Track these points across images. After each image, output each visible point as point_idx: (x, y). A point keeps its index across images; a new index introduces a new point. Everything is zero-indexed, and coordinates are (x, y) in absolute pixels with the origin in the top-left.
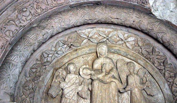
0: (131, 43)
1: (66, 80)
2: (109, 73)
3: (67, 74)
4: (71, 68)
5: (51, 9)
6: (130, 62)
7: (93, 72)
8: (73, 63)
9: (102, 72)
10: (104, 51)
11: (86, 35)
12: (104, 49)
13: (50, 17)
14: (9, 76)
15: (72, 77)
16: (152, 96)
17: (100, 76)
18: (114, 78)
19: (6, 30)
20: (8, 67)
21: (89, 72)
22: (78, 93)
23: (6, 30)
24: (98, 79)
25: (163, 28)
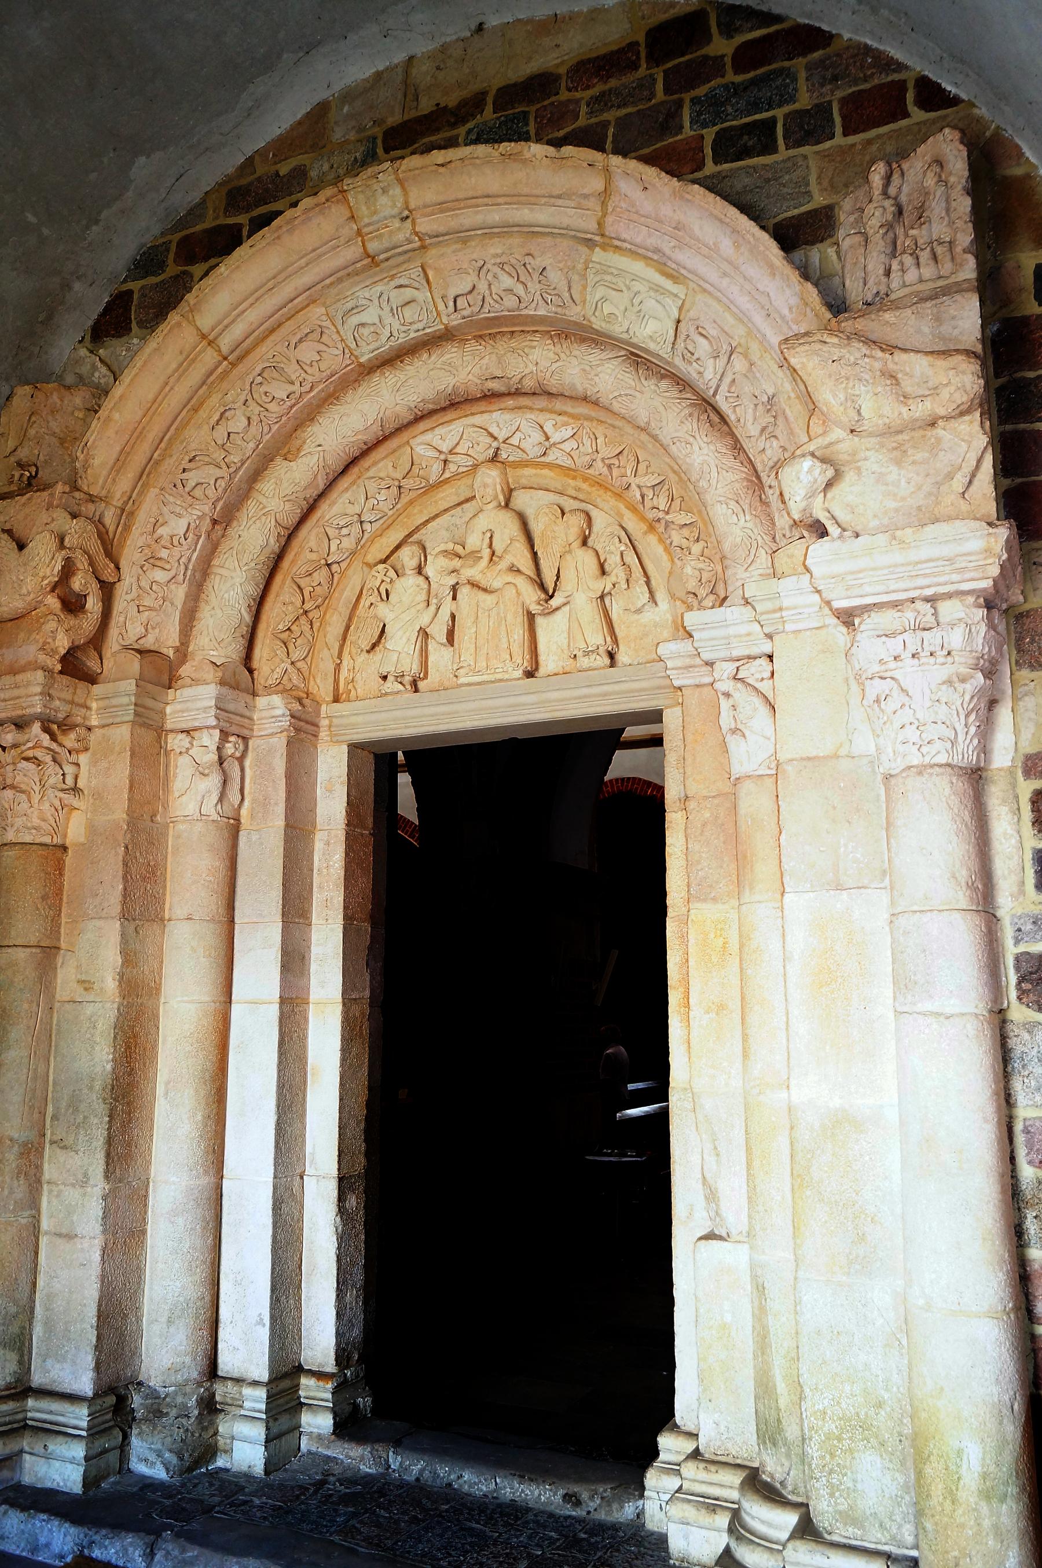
0: (567, 447)
7: (456, 563)
10: (490, 491)
12: (489, 481)
13: (310, 415)
14: (213, 612)
15: (410, 582)
23: (191, 483)
24: (474, 585)
25: (627, 380)
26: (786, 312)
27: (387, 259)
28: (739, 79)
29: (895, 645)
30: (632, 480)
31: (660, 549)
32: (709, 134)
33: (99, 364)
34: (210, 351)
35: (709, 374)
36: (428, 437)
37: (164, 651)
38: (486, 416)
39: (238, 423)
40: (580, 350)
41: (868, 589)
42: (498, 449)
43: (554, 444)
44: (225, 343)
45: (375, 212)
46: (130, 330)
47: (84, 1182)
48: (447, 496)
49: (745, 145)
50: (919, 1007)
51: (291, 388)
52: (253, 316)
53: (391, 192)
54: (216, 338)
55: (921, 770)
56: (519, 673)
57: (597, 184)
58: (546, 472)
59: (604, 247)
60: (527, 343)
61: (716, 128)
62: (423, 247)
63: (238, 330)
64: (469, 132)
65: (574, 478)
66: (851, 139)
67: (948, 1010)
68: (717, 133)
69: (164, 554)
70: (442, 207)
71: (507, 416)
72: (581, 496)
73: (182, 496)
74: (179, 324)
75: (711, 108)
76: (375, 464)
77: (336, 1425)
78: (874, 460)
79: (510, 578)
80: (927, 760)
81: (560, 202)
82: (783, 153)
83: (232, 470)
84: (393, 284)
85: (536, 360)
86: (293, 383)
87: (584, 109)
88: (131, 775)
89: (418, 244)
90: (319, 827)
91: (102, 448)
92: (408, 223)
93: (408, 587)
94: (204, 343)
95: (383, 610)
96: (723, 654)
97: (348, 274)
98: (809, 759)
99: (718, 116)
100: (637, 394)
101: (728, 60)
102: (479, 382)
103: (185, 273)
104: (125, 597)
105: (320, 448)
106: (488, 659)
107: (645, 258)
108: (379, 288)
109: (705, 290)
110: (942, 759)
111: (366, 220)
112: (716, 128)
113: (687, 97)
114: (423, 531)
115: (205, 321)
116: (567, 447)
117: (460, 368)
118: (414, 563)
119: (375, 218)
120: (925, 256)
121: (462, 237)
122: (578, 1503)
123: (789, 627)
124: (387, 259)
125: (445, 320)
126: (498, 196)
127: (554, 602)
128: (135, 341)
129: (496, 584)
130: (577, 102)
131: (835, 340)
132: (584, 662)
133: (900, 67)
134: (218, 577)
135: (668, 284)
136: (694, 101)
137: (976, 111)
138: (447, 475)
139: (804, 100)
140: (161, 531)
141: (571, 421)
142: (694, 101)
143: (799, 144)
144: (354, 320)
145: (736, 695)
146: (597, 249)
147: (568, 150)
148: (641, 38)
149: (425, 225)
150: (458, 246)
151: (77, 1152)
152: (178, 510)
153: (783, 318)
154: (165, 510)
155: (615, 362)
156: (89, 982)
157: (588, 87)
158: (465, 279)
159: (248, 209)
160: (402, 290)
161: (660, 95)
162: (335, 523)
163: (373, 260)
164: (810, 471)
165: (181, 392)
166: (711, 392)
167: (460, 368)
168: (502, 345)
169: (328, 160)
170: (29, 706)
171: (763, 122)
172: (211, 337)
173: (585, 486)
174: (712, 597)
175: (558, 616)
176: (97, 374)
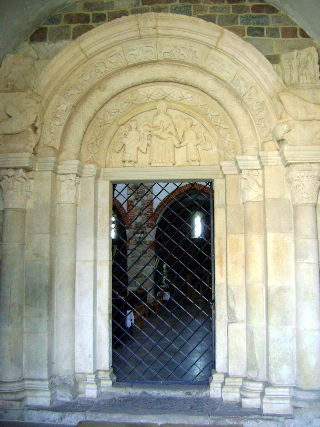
0: (189, 100)
1: (128, 137)
2: (166, 129)
3: (129, 131)
4: (133, 124)
5: (110, 71)
8: (135, 120)
10: (163, 109)
11: (145, 93)
13: (109, 77)
16: (207, 151)
17: (158, 132)
18: (171, 133)
19: (69, 94)
21: (148, 128)
22: (138, 148)
23: (69, 94)
24: (157, 136)
26: (272, 82)
27: (145, 38)
28: (254, 14)
29: (302, 173)
32: (246, 27)
33: (32, 49)
34: (83, 55)
36: (143, 89)
37: (56, 147)
38: (163, 86)
39: (87, 77)
40: (201, 75)
41: (297, 159)
42: (166, 97)
43: (185, 98)
44: (88, 53)
46: (46, 40)
47: (40, 315)
48: (147, 107)
49: (256, 33)
50: (305, 261)
51: (106, 69)
52: (100, 46)
53: (152, 21)
54: (85, 51)
55: (306, 205)
56: (172, 165)
57: (218, 35)
58: (180, 105)
59: (215, 50)
60: (184, 70)
61: (248, 26)
62: (157, 37)
63: (93, 49)
64: (172, 6)
65: (189, 109)
66: (284, 39)
67: (311, 262)
68: (248, 27)
69: (59, 116)
70: (168, 28)
71: (170, 87)
72: (190, 114)
73: (66, 98)
74: (75, 45)
75: (247, 20)
76: (124, 95)
77: (113, 384)
78: (298, 126)
79: (170, 136)
80: (308, 202)
82: (266, 38)
83: (82, 92)
85: (187, 75)
86: (106, 68)
87: (209, 10)
88: (51, 188)
90: (99, 207)
91: (44, 80)
92: (155, 30)
93: (133, 134)
94: (81, 52)
95: (124, 140)
96: (246, 168)
98: (273, 199)
99: (249, 23)
101: (250, 8)
103: (68, 26)
104: (46, 129)
106: (162, 159)
107: (227, 56)
108: (141, 45)
109: (245, 69)
110: (311, 202)
111: (142, 26)
112: (248, 26)
113: (239, 15)
114: (136, 117)
115: (83, 45)
116: (189, 100)
117: (162, 72)
118: (135, 127)
120: (308, 77)
121: (170, 36)
122: (190, 394)
123: (269, 164)
124: (145, 38)
125: (159, 58)
126: (186, 29)
127: (182, 145)
128: (47, 44)
129: (165, 137)
130: (207, 7)
131: (292, 95)
132: (192, 163)
133: (295, 24)
134: (75, 125)
135: (234, 65)
136: (241, 17)
137: (314, 41)
138: (147, 101)
139: (271, 25)
140: (58, 108)
141: (191, 93)
142: (241, 17)
143: (270, 36)
144: (130, 53)
145: (249, 179)
146: (213, 50)
149: (160, 31)
151: (36, 307)
152: (64, 102)
153: (270, 83)
154: (60, 102)
155: (212, 81)
156: (38, 254)
157: (209, 4)
159: (92, 11)
160: (148, 47)
161: (231, 13)
163: (140, 37)
164: (287, 127)
165: (70, 66)
166: (242, 95)
168: (176, 69)
169: (122, 2)
170: (23, 164)
171: (261, 28)
172: (84, 50)
173: (192, 112)
174: (233, 150)
175: (182, 149)
176: (31, 52)
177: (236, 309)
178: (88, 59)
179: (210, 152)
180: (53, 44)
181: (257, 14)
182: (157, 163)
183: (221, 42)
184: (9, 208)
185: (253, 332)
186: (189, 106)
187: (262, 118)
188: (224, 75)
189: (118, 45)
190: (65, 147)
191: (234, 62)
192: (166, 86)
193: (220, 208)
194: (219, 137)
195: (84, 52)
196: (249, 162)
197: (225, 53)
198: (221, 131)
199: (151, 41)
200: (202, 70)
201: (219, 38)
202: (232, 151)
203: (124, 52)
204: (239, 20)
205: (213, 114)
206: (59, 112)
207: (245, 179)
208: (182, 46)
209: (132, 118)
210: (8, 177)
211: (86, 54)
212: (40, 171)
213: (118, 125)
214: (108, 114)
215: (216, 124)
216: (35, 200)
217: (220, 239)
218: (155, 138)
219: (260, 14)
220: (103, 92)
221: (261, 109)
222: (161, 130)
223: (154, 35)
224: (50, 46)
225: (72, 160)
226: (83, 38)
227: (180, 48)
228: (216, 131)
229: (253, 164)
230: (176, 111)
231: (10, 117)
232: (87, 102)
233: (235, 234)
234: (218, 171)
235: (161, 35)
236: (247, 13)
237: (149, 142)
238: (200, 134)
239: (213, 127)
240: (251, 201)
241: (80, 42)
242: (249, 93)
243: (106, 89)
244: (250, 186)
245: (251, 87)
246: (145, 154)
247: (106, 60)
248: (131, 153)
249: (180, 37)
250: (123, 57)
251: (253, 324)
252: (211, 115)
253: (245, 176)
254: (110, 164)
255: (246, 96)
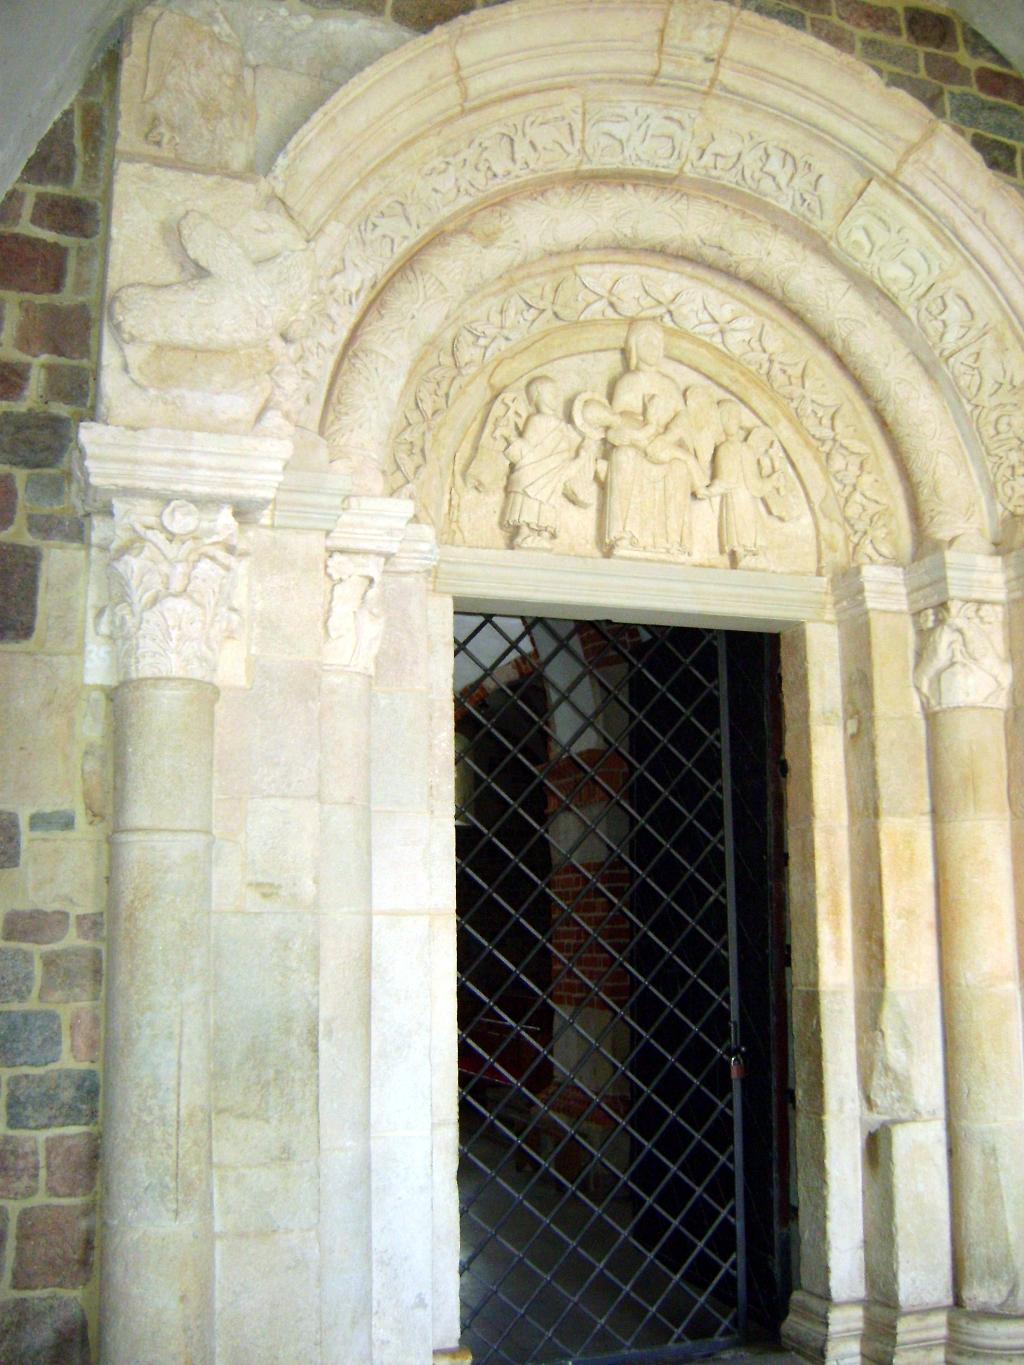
1: (529, 434)
4: (548, 395)
6: (730, 401)
9: (645, 423)
19: (379, 232)
20: (373, 371)
24: (633, 445)
27: (664, 85)
28: (983, 96)
30: (807, 394)
31: (816, 468)
34: (455, 88)
35: (951, 337)
36: (597, 269)
38: (662, 273)
44: (476, 86)
45: (689, 39)
53: (714, 31)
58: (703, 351)
59: (883, 183)
63: (495, 79)
65: (732, 368)
70: (756, 72)
72: (734, 388)
74: (441, 45)
79: (679, 454)
81: (869, 129)
84: (665, 113)
89: (703, 88)
92: (711, 66)
93: (547, 427)
96: (964, 594)
97: (624, 80)
100: (868, 325)
102: (699, 243)
105: (517, 245)
106: (654, 536)
108: (650, 109)
111: (676, 42)
113: (947, 88)
115: (466, 53)
116: (739, 336)
117: (691, 222)
119: (687, 45)
121: (749, 104)
126: (814, 92)
129: (664, 456)
135: (938, 247)
141: (752, 314)
147: (901, 93)
148: (900, 10)
149: (727, 76)
150: (740, 110)
156: (271, 885)
157: (858, 25)
158: (729, 139)
160: (668, 123)
162: (480, 329)
166: (946, 353)
167: (691, 222)
170: (255, 487)
173: (742, 379)
174: (885, 530)
177: (914, 1073)
178: (464, 113)
179: (789, 528)
180: (307, 20)
181: (991, 99)
182: (633, 544)
183: (916, 162)
184: (146, 679)
185: (994, 1150)
186: (732, 360)
187: (1011, 435)
188: (893, 274)
189: (570, 86)
190: (343, 441)
191: (938, 239)
192: (671, 275)
193: (826, 724)
194: (828, 480)
195: (461, 80)
196: (975, 576)
197: (915, 202)
198: (838, 463)
199: (682, 102)
200: (821, 247)
201: (912, 148)
202: (881, 533)
203: (588, 117)
204: (946, 98)
205: (820, 398)
206: (336, 295)
207: (960, 631)
208: (782, 146)
209: (536, 368)
210: (172, 537)
211: (466, 89)
212: (273, 527)
213: (491, 386)
214: (470, 338)
215: (827, 433)
216: (254, 650)
217: (830, 832)
218: (631, 453)
219: (1000, 101)
220: (484, 251)
221: (1009, 408)
222: (651, 430)
223: (702, 82)
224: (295, 23)
225: (373, 496)
226: (473, 24)
227: (771, 150)
228: (817, 458)
229: (988, 582)
230: (685, 369)
231: (201, 272)
232: (426, 277)
233: (903, 815)
234: (824, 597)
235: (725, 88)
236: (965, 89)
237: (602, 466)
238: (766, 462)
239: (807, 444)
240: (973, 707)
241: (463, 35)
242: (973, 349)
243: (499, 244)
244: (977, 656)
245: (985, 334)
246: (582, 511)
247: (520, 133)
248: (540, 501)
249: (781, 115)
250: (578, 135)
251: (995, 1120)
252: (813, 401)
253: (959, 622)
254: (454, 532)
255: (961, 357)
